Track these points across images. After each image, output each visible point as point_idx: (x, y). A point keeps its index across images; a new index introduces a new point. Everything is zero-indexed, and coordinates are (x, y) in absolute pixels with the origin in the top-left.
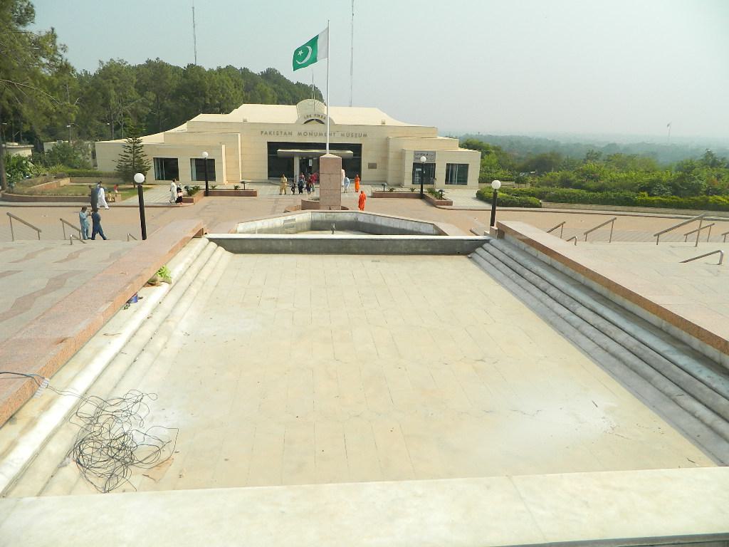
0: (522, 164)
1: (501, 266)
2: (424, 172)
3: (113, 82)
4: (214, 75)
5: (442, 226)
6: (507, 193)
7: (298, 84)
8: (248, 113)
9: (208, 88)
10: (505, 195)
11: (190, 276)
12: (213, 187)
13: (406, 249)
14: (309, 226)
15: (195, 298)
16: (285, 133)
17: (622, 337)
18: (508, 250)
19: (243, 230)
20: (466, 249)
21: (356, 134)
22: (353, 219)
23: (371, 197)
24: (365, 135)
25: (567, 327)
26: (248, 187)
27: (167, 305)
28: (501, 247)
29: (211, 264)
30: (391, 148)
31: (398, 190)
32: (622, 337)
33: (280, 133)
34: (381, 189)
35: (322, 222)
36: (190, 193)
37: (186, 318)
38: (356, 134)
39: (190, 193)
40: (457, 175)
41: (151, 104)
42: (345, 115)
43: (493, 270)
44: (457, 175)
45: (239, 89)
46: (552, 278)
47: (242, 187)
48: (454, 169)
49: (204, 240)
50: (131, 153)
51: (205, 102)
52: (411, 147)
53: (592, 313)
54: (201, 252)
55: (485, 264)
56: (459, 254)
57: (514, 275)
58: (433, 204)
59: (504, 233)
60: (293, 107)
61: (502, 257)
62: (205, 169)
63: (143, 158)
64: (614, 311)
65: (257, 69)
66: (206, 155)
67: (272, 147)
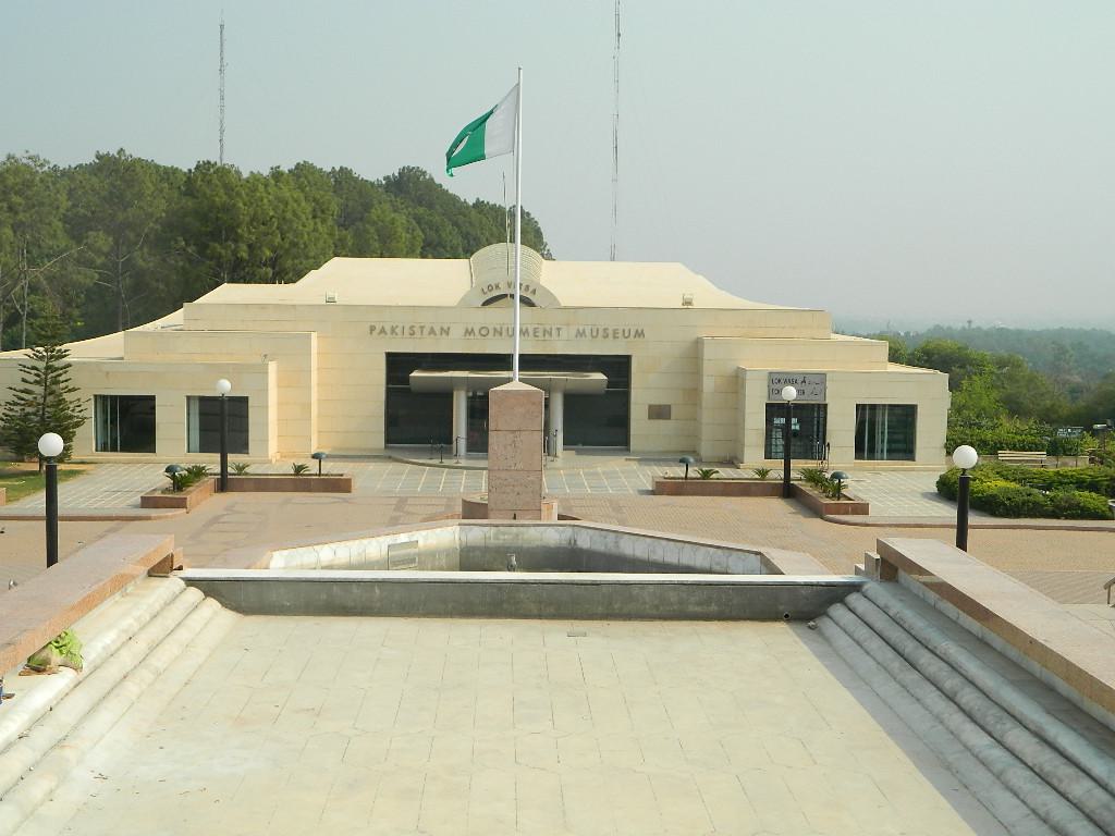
0: (1066, 407)
1: (875, 644)
2: (797, 426)
3: (10, 209)
4: (261, 188)
5: (776, 556)
6: (1020, 481)
7: (479, 205)
8: (345, 280)
9: (247, 219)
10: (1013, 485)
11: (127, 658)
12: (240, 469)
13: (657, 607)
14: (457, 560)
15: (133, 704)
16: (432, 331)
17: (1080, 788)
18: (896, 607)
19: (282, 564)
20: (805, 608)
22: (564, 543)
23: (653, 493)
24: (639, 334)
25: (980, 776)
26: (330, 467)
27: (67, 715)
28: (881, 602)
29: (183, 635)
30: (709, 368)
31: (724, 473)
32: (1080, 788)
34: (679, 471)
35: (486, 549)
36: (180, 483)
37: (106, 742)
39: (180, 483)
40: (886, 432)
41: (99, 261)
42: (588, 287)
43: (855, 654)
44: (886, 432)
45: (324, 221)
46: (972, 667)
47: (313, 467)
48: (879, 419)
49: (174, 582)
50: (36, 382)
51: (235, 252)
52: (759, 362)
53: (1036, 740)
54: (162, 609)
55: (842, 641)
56: (787, 618)
57: (896, 664)
58: (816, 511)
59: (897, 570)
60: (460, 265)
61: (880, 622)
62: (222, 422)
63: (68, 397)
64: (1082, 735)
65: (374, 169)
66: (225, 387)
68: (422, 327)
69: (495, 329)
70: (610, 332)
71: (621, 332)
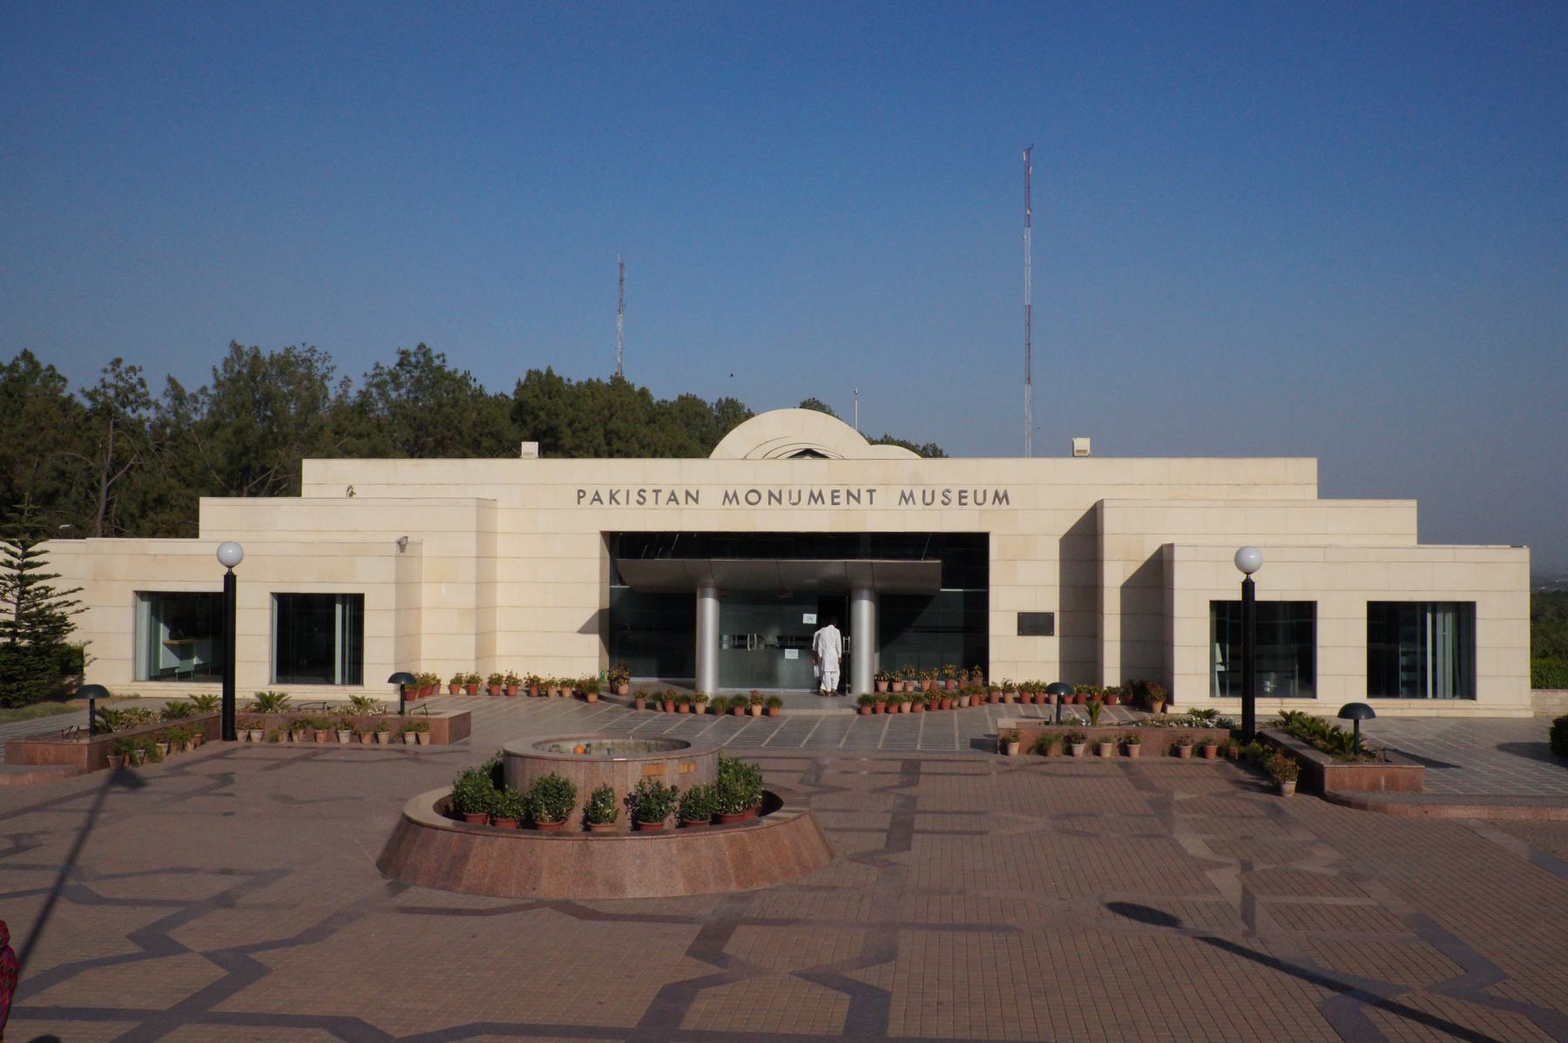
16: (673, 498)
21: (962, 495)
24: (1002, 498)
33: (650, 496)
38: (962, 495)
67: (623, 546)
68: (657, 492)
69: (771, 494)
70: (954, 496)
71: (970, 495)
